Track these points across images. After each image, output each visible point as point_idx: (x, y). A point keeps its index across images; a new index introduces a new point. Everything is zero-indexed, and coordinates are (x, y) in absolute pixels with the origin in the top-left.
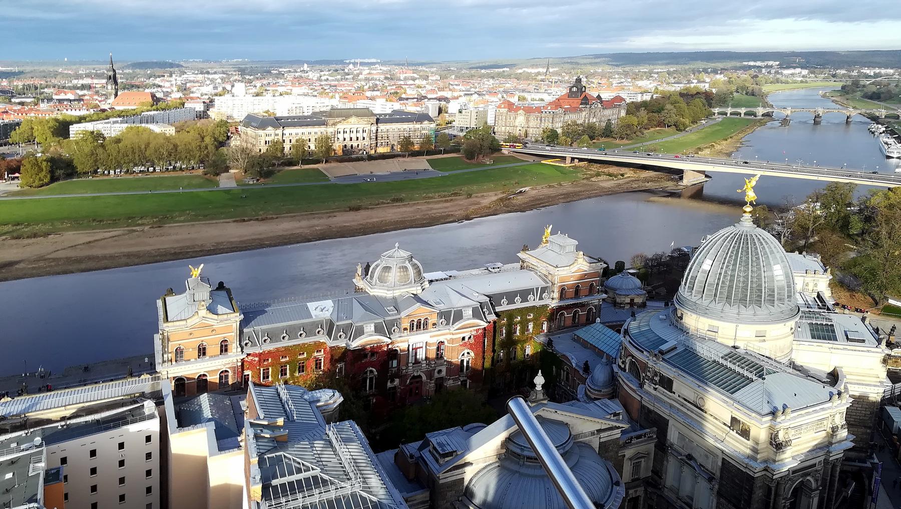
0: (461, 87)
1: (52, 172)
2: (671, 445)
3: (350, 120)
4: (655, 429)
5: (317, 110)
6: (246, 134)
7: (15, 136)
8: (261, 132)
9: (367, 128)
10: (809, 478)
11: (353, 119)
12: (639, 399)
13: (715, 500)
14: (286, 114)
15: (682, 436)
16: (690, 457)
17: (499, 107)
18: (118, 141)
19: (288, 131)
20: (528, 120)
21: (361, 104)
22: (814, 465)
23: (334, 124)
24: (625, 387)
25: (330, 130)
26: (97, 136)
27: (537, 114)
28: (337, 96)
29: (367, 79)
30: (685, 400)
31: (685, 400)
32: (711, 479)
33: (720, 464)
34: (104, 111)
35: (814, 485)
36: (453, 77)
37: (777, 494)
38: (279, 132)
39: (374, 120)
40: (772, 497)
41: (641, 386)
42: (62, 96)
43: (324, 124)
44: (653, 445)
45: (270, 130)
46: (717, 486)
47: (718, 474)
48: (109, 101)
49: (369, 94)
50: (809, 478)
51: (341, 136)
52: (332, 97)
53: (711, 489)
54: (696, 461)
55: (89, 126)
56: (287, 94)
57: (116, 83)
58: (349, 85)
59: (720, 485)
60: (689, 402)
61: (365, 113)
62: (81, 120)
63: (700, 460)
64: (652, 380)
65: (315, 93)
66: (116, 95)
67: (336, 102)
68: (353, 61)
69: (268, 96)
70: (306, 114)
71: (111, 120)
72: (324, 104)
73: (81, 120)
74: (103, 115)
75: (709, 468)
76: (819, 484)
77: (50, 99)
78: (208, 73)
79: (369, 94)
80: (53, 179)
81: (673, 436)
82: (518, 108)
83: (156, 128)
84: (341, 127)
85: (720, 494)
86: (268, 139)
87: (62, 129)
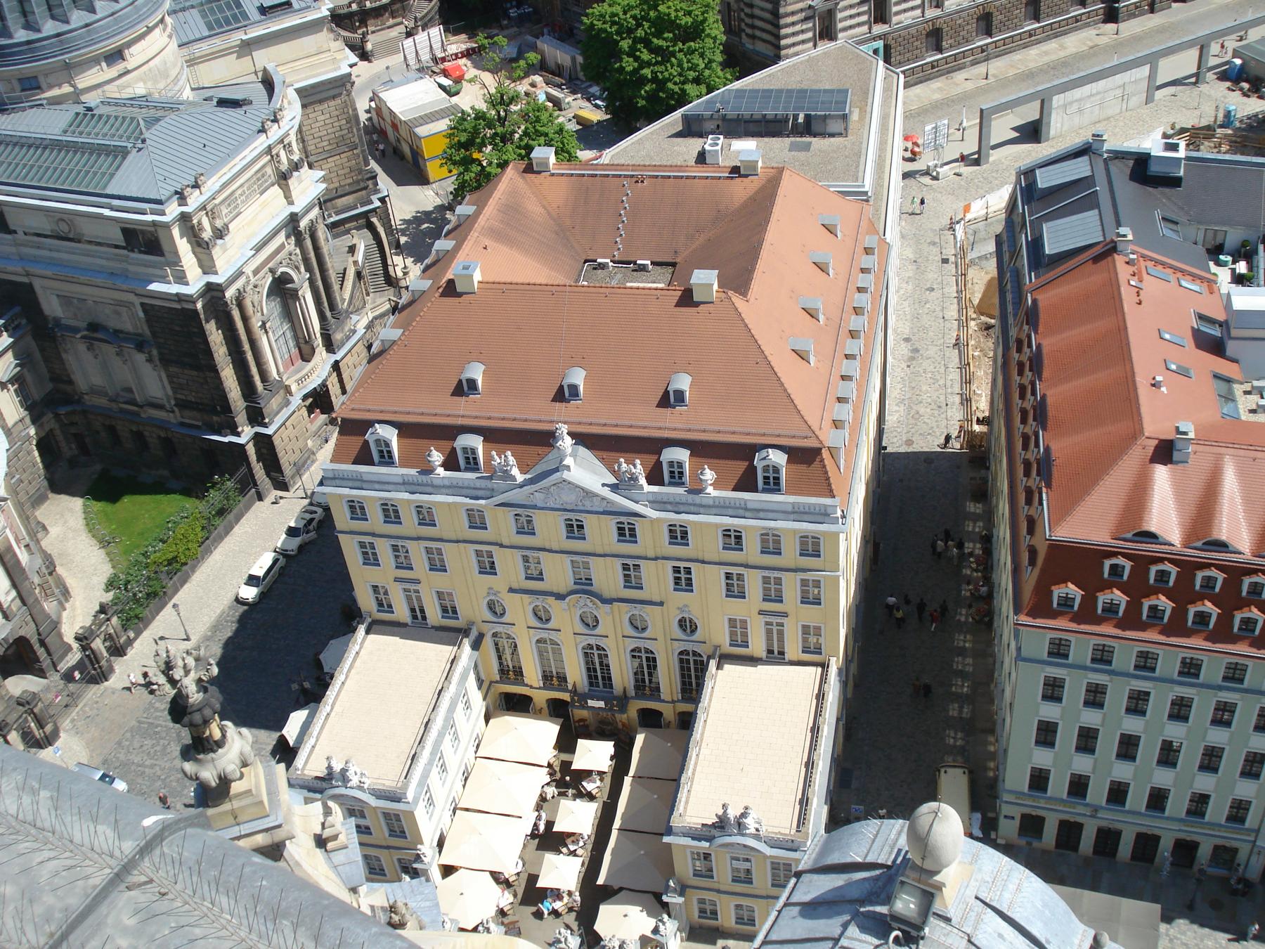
2: (57, 321)
4: (17, 309)
15: (65, 300)
16: (94, 327)
30: (38, 235)
31: (38, 235)
32: (140, 346)
37: (245, 319)
44: (29, 339)
46: (155, 352)
47: (147, 332)
50: (282, 270)
53: (150, 360)
60: (46, 236)
63: (113, 323)
75: (128, 327)
81: (52, 306)
85: (165, 361)
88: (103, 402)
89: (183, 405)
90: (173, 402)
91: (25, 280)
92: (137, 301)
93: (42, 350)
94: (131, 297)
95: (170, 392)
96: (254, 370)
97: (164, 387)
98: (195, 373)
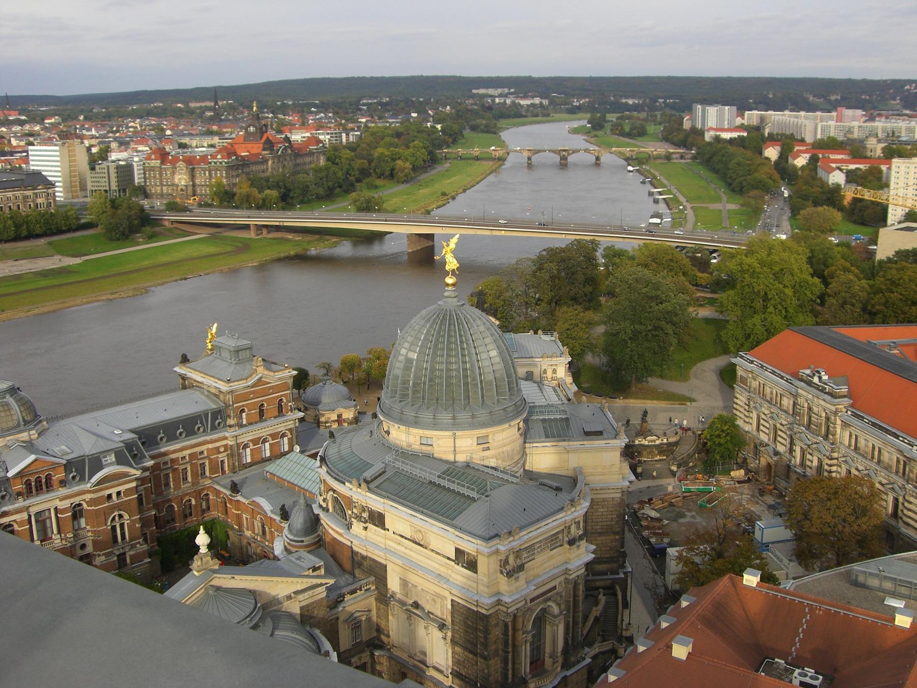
0: (94, 132)
4: (372, 579)
10: (550, 603)
12: (349, 544)
13: (450, 651)
15: (404, 583)
16: (416, 605)
17: (149, 158)
20: (193, 177)
22: (554, 588)
24: (330, 531)
27: (203, 165)
30: (402, 536)
31: (402, 536)
32: (442, 627)
33: (449, 607)
35: (556, 610)
36: (82, 118)
37: (515, 630)
40: (510, 633)
41: (349, 527)
44: (373, 599)
46: (449, 634)
47: (449, 619)
54: (423, 609)
59: (453, 631)
60: (406, 538)
64: (359, 518)
75: (438, 613)
76: (563, 607)
81: (393, 584)
82: (176, 159)
85: (454, 642)
88: (405, 656)
89: (456, 674)
90: (450, 671)
91: (384, 562)
92: (450, 597)
93: (378, 609)
94: (447, 594)
95: (450, 663)
96: (510, 666)
97: (447, 659)
98: (471, 656)
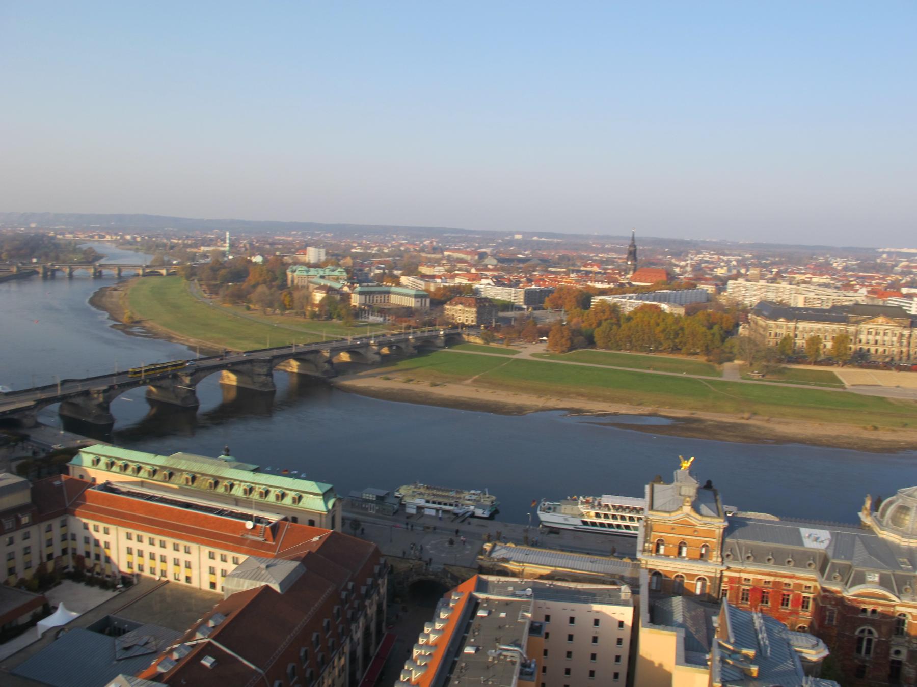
1: (571, 339)
3: (876, 319)
5: (839, 304)
6: (756, 323)
7: (547, 302)
8: (771, 323)
9: (898, 330)
11: (881, 319)
14: (801, 305)
18: (629, 318)
19: (801, 325)
21: (893, 301)
23: (857, 323)
25: (852, 329)
26: (614, 309)
28: (864, 291)
29: (903, 274)
34: (622, 285)
38: (792, 324)
39: (907, 322)
42: (588, 268)
43: (845, 321)
45: (782, 322)
48: (628, 276)
49: (904, 290)
51: (863, 337)
52: (856, 291)
55: (608, 298)
56: (804, 282)
57: (635, 259)
58: (880, 279)
61: (897, 314)
62: (603, 292)
65: (839, 284)
66: (635, 271)
67: (861, 295)
68: (887, 250)
69: (784, 285)
70: (825, 307)
71: (628, 295)
72: (846, 299)
73: (603, 292)
74: (621, 289)
77: (578, 271)
78: (725, 255)
79: (904, 290)
80: (572, 348)
83: (664, 306)
84: (864, 326)
86: (778, 331)
87: (584, 300)
